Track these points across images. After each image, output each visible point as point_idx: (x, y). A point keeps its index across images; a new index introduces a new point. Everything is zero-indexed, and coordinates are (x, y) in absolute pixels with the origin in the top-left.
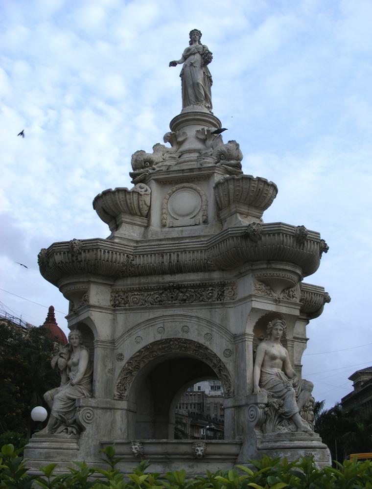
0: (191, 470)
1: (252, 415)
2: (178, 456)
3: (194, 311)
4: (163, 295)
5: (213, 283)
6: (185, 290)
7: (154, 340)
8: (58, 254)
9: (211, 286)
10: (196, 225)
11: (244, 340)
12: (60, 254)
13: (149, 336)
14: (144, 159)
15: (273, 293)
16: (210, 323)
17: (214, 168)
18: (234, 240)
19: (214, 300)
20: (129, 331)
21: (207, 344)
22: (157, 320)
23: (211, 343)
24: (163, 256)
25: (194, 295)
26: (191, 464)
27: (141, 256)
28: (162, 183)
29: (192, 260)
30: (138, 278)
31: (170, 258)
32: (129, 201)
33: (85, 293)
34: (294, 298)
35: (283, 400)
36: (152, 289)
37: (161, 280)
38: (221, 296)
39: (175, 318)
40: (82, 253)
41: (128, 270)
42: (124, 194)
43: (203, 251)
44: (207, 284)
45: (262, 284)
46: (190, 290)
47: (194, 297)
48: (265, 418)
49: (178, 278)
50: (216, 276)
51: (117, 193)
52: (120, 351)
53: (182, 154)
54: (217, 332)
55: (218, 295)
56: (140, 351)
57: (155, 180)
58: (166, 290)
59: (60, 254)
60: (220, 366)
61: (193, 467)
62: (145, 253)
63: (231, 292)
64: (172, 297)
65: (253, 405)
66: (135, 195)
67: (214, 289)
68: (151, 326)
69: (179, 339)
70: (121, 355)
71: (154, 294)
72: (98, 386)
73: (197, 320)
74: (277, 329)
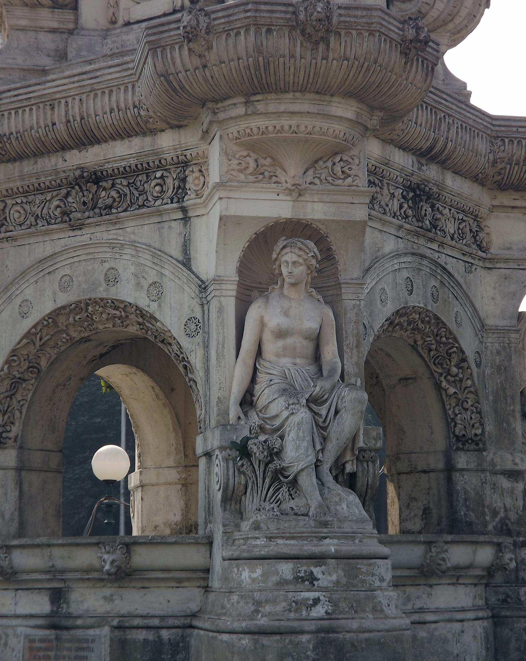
15: (279, 172)
16: (158, 254)
21: (153, 308)
22: (59, 259)
23: (159, 306)
25: (128, 193)
26: (108, 592)
30: (17, 164)
34: (349, 180)
35: (282, 437)
37: (61, 165)
38: (181, 191)
39: (92, 250)
45: (249, 155)
48: (243, 482)
49: (91, 157)
50: (167, 142)
54: (172, 277)
61: (113, 600)
63: (197, 178)
69: (102, 300)
71: (52, 198)
73: (133, 253)
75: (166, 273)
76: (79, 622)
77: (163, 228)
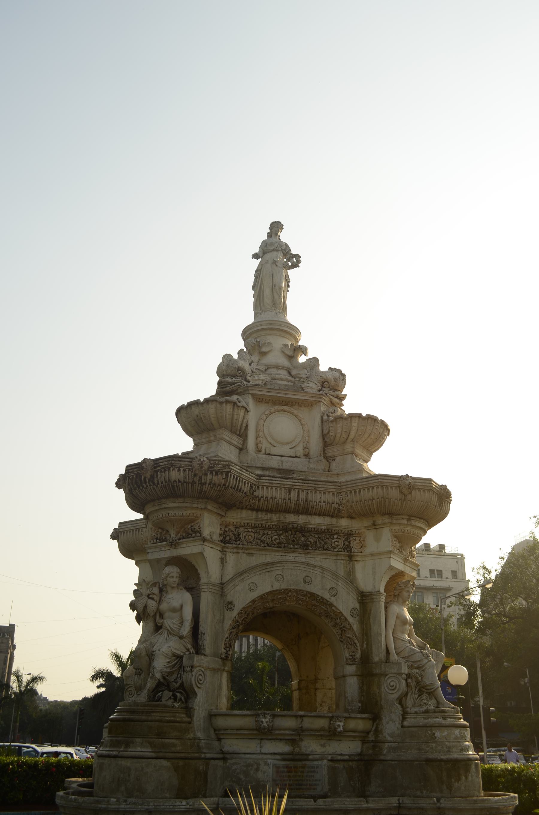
0: (323, 750)
1: (392, 686)
2: (313, 733)
3: (318, 559)
4: (282, 537)
5: (340, 531)
6: (308, 534)
7: (272, 590)
8: (177, 470)
9: (337, 533)
10: (296, 457)
11: (379, 599)
12: (179, 470)
13: (265, 584)
14: (239, 367)
16: (335, 575)
17: (321, 396)
18: (383, 490)
19: (340, 550)
20: (240, 574)
21: (332, 600)
22: (276, 565)
24: (290, 493)
26: (323, 742)
27: (279, 489)
28: (259, 400)
29: (322, 502)
30: (255, 512)
31: (298, 495)
32: (235, 417)
33: (192, 522)
35: (424, 671)
36: (271, 528)
37: (282, 519)
39: (297, 565)
40: (209, 474)
41: (248, 501)
42: (232, 407)
43: (336, 494)
44: (333, 531)
46: (313, 534)
47: (318, 543)
49: (302, 519)
51: (224, 404)
52: (229, 598)
53: (268, 368)
54: (343, 587)
55: (344, 544)
56: (254, 601)
57: (253, 395)
58: (287, 532)
59: (179, 470)
60: (344, 627)
61: (325, 746)
62: (271, 485)
64: (294, 541)
65: (392, 675)
66: (243, 411)
67: (339, 537)
68: (268, 571)
69: (300, 590)
70: (231, 603)
72: (207, 641)
73: (321, 571)
74: (408, 591)
75: (340, 584)
76: (311, 757)
77: (337, 562)
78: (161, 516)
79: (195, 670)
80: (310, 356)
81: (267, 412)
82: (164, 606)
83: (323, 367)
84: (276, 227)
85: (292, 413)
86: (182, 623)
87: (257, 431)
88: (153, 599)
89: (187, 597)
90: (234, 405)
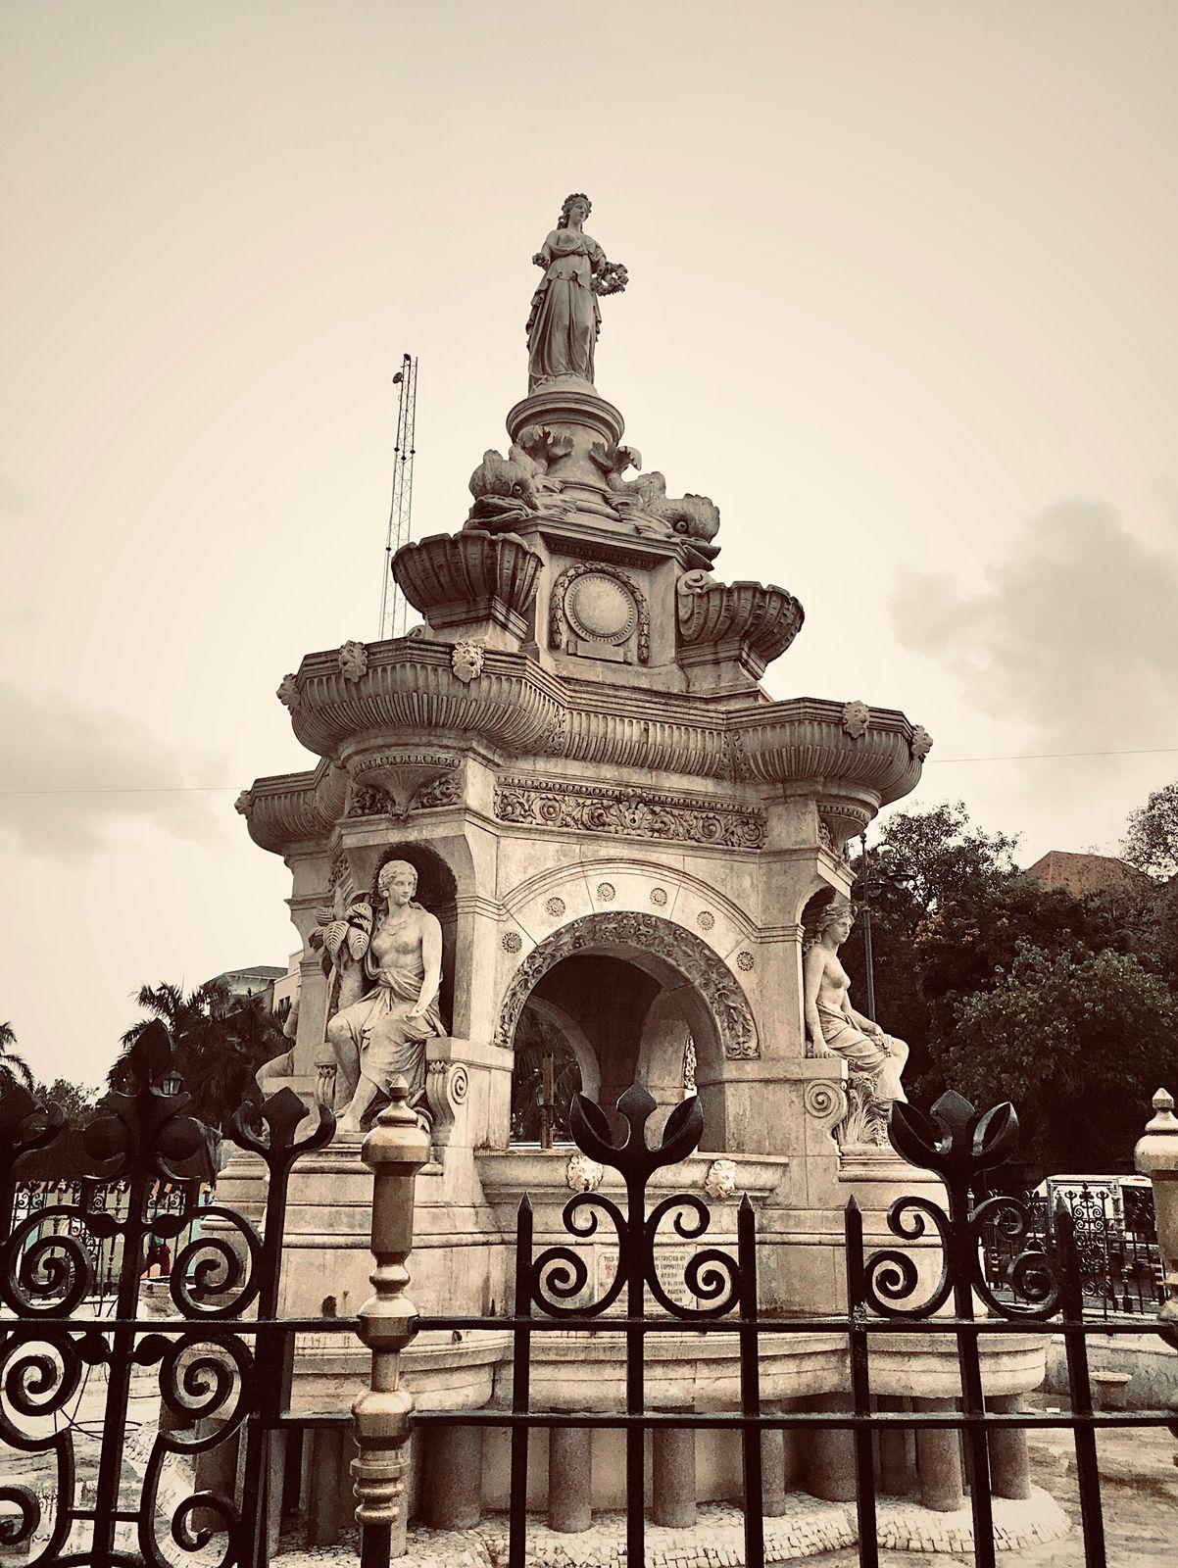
1: (819, 1103)
13: (581, 902)
19: (718, 841)
28: (557, 546)
41: (551, 739)
63: (753, 830)
78: (379, 761)
79: (452, 1070)
80: (647, 468)
81: (572, 572)
82: (382, 942)
83: (674, 492)
84: (575, 208)
85: (615, 576)
86: (421, 975)
87: (552, 610)
88: (360, 927)
89: (432, 924)
90: (517, 550)
